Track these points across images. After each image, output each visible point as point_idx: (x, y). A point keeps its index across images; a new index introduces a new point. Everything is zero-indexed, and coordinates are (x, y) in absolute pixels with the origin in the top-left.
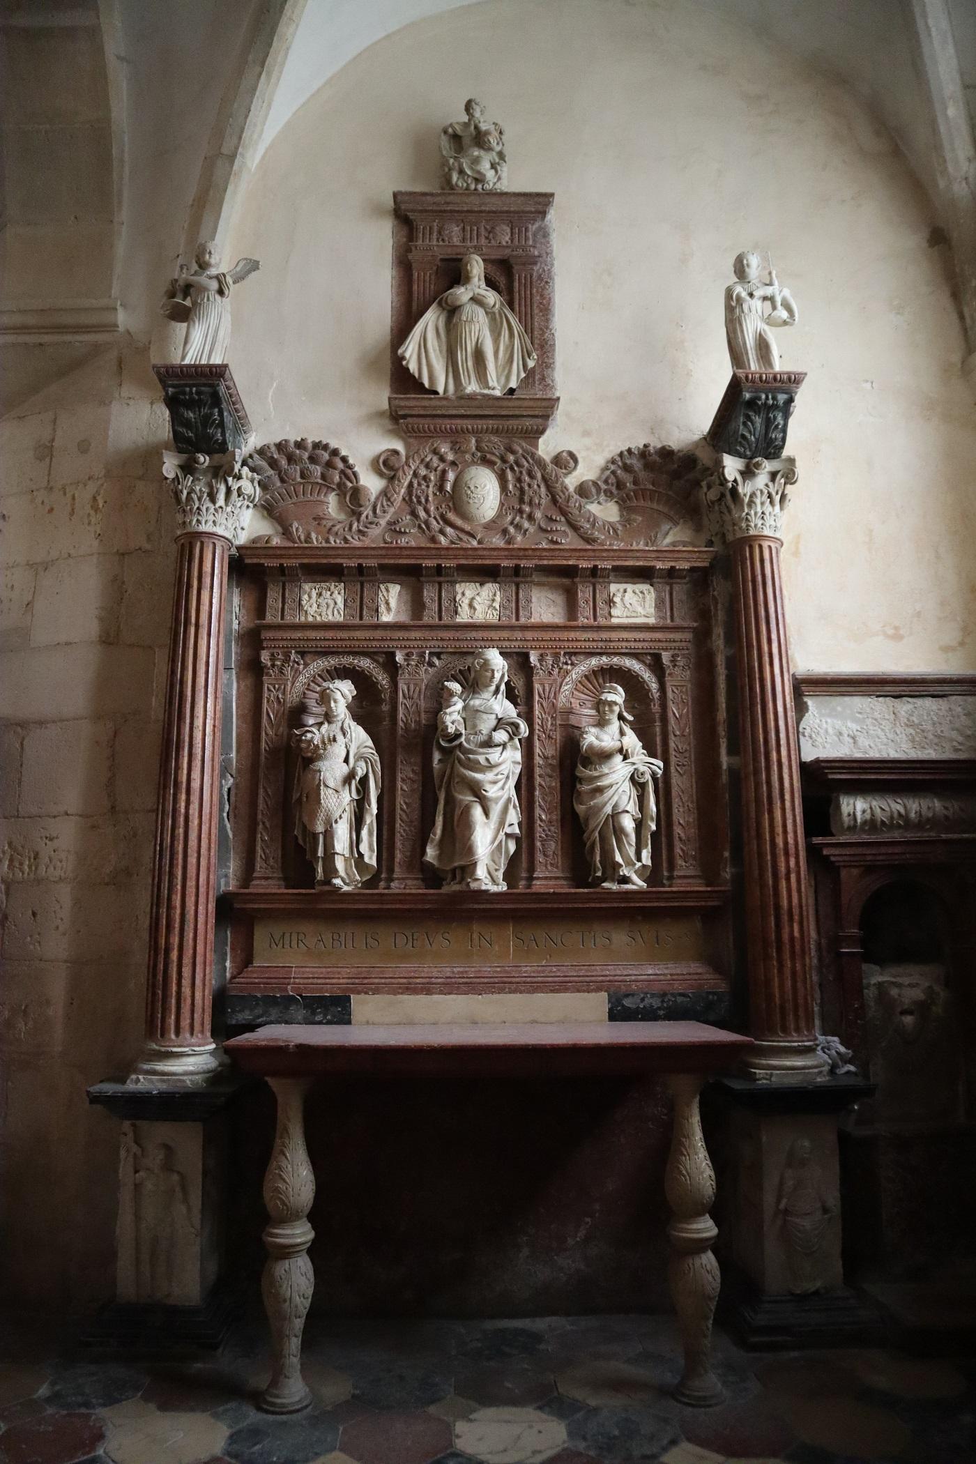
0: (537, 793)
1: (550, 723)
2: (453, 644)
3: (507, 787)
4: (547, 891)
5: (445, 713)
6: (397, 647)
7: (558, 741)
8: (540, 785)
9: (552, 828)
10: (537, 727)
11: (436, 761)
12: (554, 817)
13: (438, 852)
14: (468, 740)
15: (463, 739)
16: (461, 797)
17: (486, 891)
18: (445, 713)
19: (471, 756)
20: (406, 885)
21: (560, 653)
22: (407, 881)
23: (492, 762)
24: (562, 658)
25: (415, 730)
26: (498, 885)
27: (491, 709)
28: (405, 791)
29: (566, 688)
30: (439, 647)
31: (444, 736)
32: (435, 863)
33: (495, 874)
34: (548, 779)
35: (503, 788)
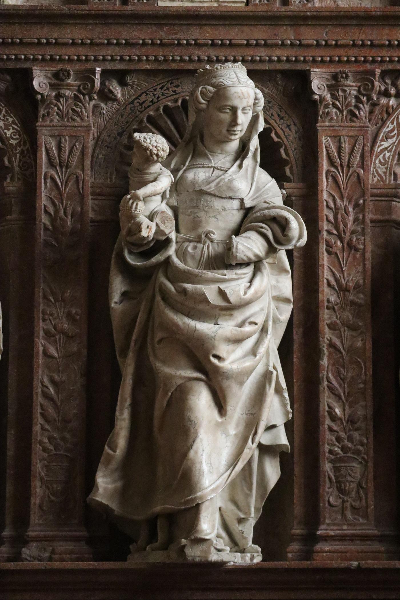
0: (325, 362)
1: (351, 218)
2: (153, 53)
3: (262, 350)
4: (343, 564)
5: (136, 198)
6: (35, 60)
7: (368, 255)
8: (331, 345)
9: (356, 435)
10: (325, 226)
11: (116, 297)
12: (360, 413)
13: (119, 484)
14: (182, 254)
15: (171, 251)
16: (167, 370)
17: (220, 565)
18: (136, 198)
19: (188, 286)
20: (53, 552)
21: (373, 74)
22: (55, 544)
23: (232, 299)
24: (376, 83)
25: (73, 232)
26: (243, 551)
27: (230, 188)
28: (52, 357)
29: (385, 144)
30: (122, 60)
31: (133, 244)
32: (114, 505)
33: (236, 528)
34: (347, 333)
35: (254, 352)
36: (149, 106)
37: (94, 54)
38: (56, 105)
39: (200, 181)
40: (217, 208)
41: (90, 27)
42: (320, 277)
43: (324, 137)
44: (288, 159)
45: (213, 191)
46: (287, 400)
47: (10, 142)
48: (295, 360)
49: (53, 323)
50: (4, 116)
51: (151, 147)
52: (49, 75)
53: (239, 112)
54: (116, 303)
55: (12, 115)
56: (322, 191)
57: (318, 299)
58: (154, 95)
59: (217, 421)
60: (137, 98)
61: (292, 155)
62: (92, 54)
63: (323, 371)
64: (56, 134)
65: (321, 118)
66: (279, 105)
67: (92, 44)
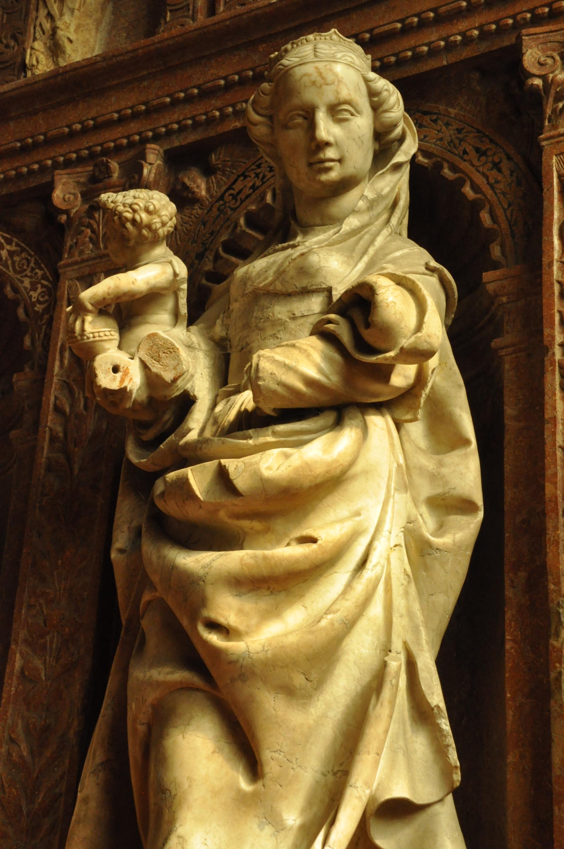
30: (196, 125)
36: (248, 196)
37: (152, 127)
38: (89, 226)
39: (254, 274)
40: (279, 316)
41: (145, 83)
42: (548, 449)
43: (555, 158)
44: (495, 226)
45: (271, 283)
46: (445, 737)
47: (36, 309)
48: (508, 646)
49: (45, 611)
50: (33, 269)
51: (121, 208)
52: (82, 180)
53: (322, 117)
54: (121, 551)
55: (43, 265)
56: (551, 264)
57: (544, 495)
58: (257, 175)
59: (239, 791)
60: (230, 188)
61: (502, 218)
62: (149, 127)
63: (557, 665)
64: (87, 272)
65: (549, 122)
66: (479, 131)
67: (148, 112)
